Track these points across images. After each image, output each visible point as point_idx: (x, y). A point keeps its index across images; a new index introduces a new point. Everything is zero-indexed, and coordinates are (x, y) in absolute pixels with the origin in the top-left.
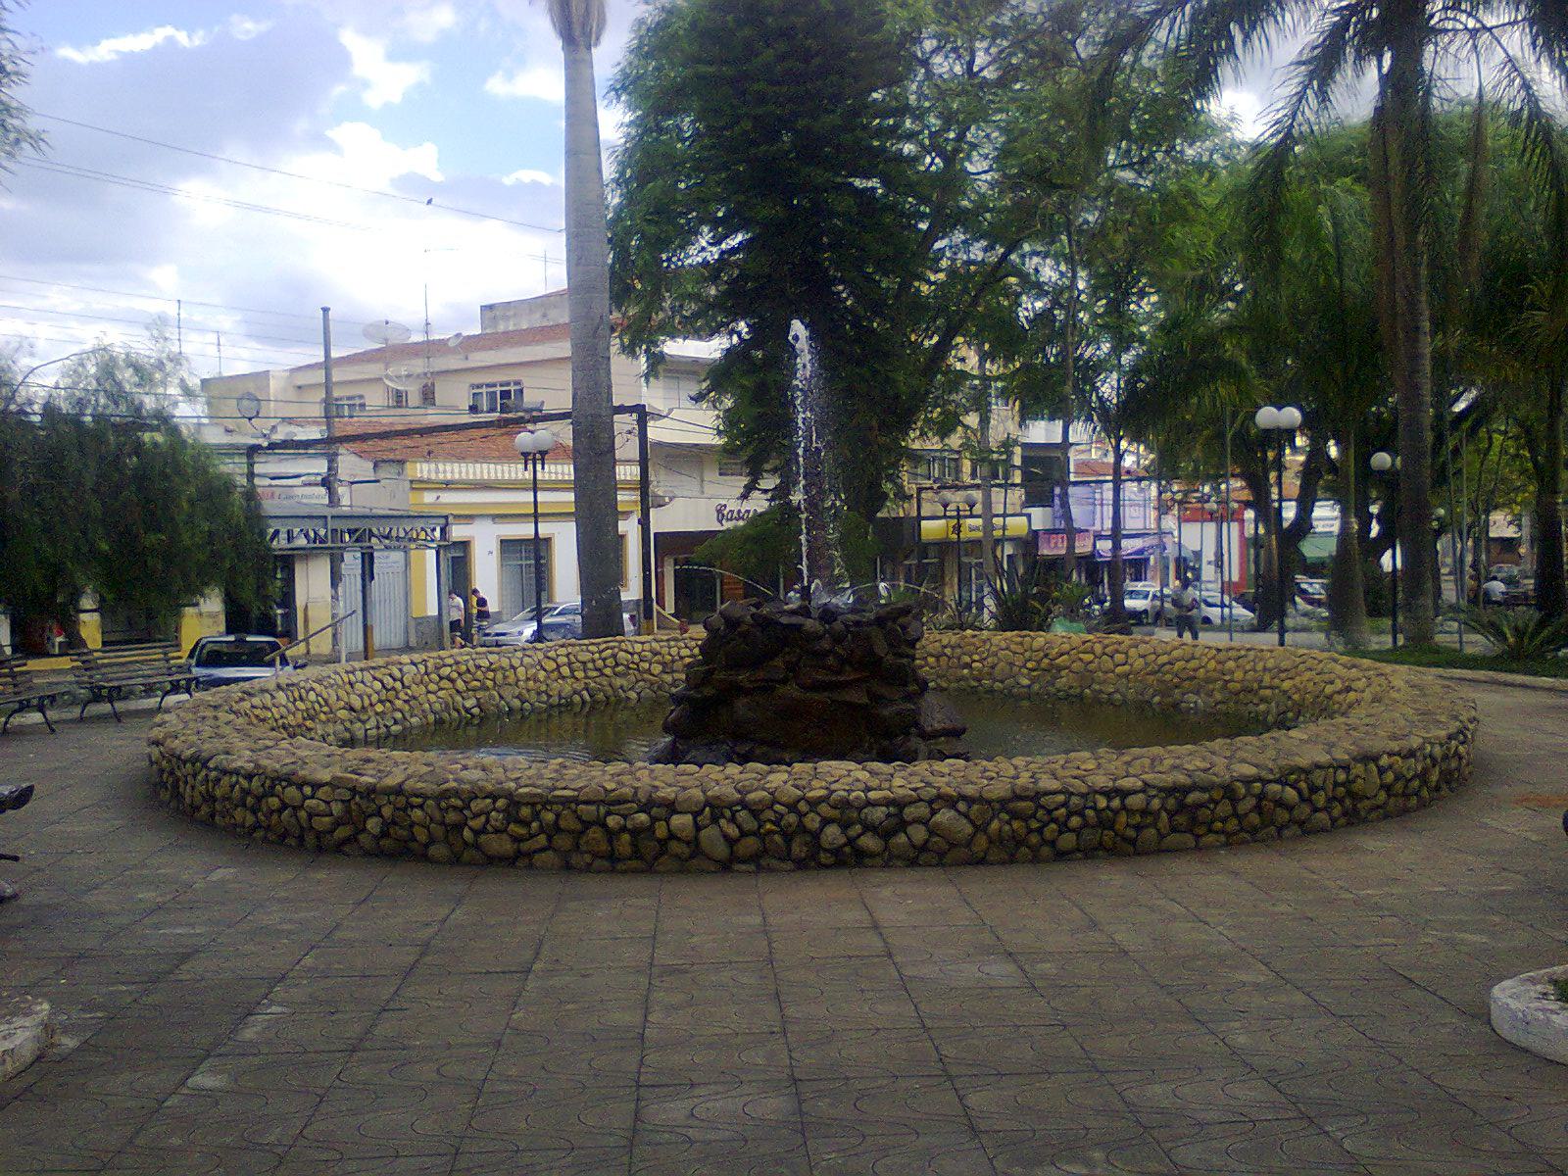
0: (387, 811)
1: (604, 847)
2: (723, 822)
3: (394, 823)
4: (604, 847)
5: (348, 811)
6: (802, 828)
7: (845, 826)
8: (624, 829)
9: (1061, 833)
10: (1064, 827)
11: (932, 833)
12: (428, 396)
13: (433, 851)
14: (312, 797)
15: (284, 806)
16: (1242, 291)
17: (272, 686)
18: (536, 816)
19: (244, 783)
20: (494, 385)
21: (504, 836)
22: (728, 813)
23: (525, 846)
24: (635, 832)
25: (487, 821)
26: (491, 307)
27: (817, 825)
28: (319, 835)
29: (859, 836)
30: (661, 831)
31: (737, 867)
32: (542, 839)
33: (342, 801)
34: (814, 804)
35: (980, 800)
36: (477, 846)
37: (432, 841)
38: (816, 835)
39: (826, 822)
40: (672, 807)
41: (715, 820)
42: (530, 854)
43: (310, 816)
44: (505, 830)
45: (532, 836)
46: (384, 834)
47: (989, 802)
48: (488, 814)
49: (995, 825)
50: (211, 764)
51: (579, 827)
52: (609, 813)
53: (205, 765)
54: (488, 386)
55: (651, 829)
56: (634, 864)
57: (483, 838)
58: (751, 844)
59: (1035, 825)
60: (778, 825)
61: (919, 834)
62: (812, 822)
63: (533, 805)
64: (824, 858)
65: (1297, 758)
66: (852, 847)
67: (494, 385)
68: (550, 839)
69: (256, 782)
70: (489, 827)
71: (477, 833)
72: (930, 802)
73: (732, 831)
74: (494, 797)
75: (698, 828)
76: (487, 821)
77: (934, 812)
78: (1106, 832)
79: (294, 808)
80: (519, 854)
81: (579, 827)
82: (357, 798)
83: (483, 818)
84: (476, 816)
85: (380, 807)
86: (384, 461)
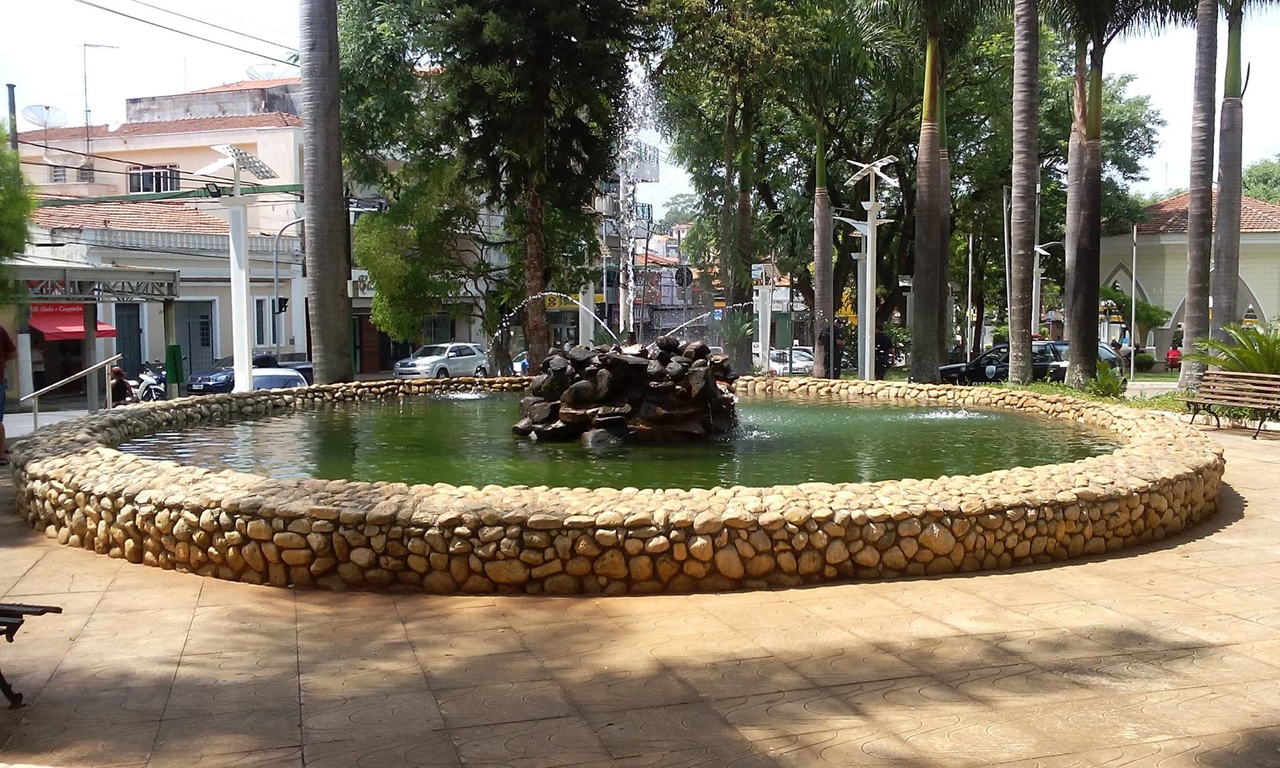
0: (378, 542)
1: (622, 572)
2: (738, 542)
3: (385, 553)
4: (622, 572)
5: (330, 542)
6: (809, 546)
7: (847, 543)
8: (643, 552)
9: (1019, 541)
10: (1023, 537)
11: (921, 547)
12: (86, 173)
13: (433, 579)
14: (285, 530)
15: (246, 539)
16: (860, 83)
17: (124, 418)
18: (551, 543)
19: (193, 518)
20: (152, 168)
21: (516, 563)
22: (744, 534)
23: (537, 572)
24: (654, 556)
25: (498, 548)
26: (134, 101)
27: (825, 542)
28: (287, 568)
29: (860, 550)
30: (679, 552)
31: (750, 583)
32: (556, 566)
33: (323, 533)
34: (822, 523)
35: (959, 514)
36: (483, 574)
37: (430, 569)
38: (822, 552)
39: (832, 539)
40: (688, 530)
41: (731, 541)
42: (541, 580)
43: (280, 550)
44: (518, 558)
45: (546, 562)
46: (375, 564)
47: (968, 516)
48: (498, 542)
49: (972, 538)
50: (140, 499)
51: (596, 552)
52: (626, 537)
53: (131, 500)
54: (146, 167)
55: (670, 552)
56: (649, 585)
57: (488, 566)
58: (765, 563)
59: (1000, 535)
60: (790, 544)
61: (910, 548)
62: (820, 539)
63: (547, 531)
64: (830, 571)
65: (541, 450)
66: (852, 561)
67: (152, 168)
68: (564, 563)
69: (206, 517)
70: (498, 554)
71: (483, 560)
72: (921, 518)
73: (748, 551)
74: (506, 524)
75: (715, 549)
76: (498, 548)
77: (924, 527)
78: (1050, 540)
79: (259, 542)
80: (530, 579)
81: (596, 552)
82: (341, 530)
83: (492, 547)
84: (486, 543)
85: (369, 539)
86: (64, 229)
